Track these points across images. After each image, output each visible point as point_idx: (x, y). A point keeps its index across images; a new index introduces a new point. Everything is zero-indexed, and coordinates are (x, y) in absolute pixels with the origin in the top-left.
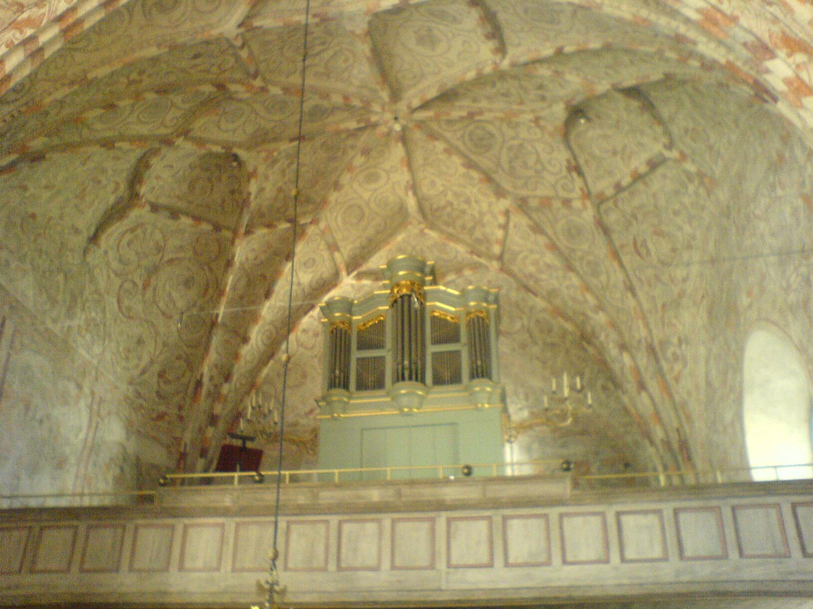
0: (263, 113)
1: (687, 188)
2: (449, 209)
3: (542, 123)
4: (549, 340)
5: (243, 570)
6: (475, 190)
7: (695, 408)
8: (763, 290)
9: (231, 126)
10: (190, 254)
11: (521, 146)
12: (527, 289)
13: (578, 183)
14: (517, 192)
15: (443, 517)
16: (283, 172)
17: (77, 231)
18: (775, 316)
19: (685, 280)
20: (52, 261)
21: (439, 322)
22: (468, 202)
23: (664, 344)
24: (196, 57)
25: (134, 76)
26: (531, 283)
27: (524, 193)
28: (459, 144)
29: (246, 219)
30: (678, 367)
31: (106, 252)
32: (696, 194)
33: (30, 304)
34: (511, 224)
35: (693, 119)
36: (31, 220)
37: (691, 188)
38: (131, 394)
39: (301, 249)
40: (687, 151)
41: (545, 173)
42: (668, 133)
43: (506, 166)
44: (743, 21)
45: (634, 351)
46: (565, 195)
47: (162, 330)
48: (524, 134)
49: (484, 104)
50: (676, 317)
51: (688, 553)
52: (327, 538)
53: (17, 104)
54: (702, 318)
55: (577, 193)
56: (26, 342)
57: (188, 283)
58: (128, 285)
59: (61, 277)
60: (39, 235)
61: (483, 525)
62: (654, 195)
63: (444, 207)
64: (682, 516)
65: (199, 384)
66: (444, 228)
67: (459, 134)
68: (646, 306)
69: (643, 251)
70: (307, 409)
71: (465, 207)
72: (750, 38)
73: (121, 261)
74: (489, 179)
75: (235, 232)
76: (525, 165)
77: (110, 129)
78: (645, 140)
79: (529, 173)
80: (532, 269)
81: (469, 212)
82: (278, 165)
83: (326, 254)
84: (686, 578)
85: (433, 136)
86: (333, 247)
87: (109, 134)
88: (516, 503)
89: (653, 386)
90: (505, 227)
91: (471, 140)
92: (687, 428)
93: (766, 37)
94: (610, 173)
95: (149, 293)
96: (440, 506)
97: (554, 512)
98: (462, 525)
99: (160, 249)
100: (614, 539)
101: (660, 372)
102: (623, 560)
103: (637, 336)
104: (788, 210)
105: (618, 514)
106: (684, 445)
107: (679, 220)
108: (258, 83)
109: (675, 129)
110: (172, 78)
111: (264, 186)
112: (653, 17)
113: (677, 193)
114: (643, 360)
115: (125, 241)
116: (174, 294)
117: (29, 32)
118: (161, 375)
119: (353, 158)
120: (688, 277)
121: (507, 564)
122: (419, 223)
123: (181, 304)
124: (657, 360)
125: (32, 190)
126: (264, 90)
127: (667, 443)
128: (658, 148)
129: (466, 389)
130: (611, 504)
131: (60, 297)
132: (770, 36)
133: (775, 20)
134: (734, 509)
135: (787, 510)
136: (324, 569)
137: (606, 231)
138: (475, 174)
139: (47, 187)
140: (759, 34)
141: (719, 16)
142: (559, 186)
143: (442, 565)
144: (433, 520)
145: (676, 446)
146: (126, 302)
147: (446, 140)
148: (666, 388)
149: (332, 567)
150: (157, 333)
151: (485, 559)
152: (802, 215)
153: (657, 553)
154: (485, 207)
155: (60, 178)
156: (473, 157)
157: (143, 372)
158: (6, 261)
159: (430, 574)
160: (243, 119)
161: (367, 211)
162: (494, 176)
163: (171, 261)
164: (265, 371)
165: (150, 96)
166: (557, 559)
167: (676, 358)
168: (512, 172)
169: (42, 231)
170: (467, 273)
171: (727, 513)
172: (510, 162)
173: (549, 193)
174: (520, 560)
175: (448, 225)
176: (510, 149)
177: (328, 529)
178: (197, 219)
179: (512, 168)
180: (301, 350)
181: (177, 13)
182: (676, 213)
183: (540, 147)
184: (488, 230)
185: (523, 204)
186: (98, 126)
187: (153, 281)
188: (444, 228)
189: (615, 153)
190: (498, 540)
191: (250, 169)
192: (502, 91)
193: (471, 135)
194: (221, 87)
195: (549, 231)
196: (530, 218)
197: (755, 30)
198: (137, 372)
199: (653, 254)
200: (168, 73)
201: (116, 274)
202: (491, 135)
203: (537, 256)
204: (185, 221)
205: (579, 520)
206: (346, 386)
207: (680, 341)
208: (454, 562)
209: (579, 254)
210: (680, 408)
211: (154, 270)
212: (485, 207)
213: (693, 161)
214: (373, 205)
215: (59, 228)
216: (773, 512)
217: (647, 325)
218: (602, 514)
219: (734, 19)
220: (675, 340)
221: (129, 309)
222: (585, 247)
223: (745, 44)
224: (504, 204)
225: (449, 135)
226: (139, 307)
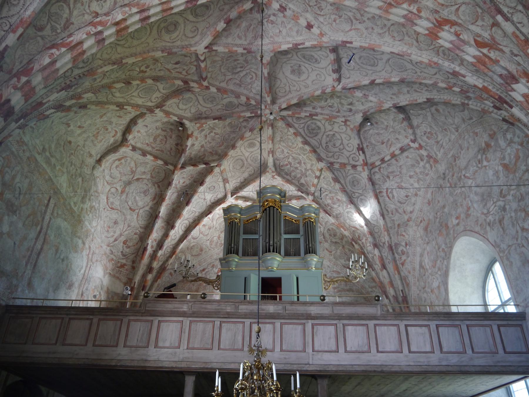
0: (202, 102)
1: (419, 164)
2: (289, 166)
3: (348, 123)
4: (334, 240)
5: (193, 349)
6: (305, 157)
7: (411, 280)
8: (468, 216)
9: (184, 107)
10: (149, 177)
11: (334, 134)
13: (362, 157)
14: (328, 159)
15: (310, 323)
16: (206, 136)
17: (91, 156)
18: (477, 229)
19: (411, 212)
20: (77, 170)
21: (288, 222)
22: (300, 163)
24: (177, 63)
25: (143, 68)
27: (332, 160)
28: (301, 131)
29: (182, 160)
30: (404, 258)
31: (104, 170)
32: (424, 167)
33: (63, 191)
34: (322, 177)
35: (431, 127)
36: (68, 144)
37: (422, 164)
38: (108, 252)
39: (209, 180)
40: (423, 144)
41: (344, 150)
42: (414, 133)
43: (324, 145)
44: (502, 63)
45: (381, 248)
46: (354, 163)
47: (128, 217)
48: (336, 128)
49: (319, 110)
50: (405, 231)
51: (445, 350)
52: (244, 332)
53: (83, 70)
54: (420, 232)
56: (60, 213)
57: (145, 192)
58: (113, 190)
59: (80, 180)
60: (72, 154)
61: (332, 329)
62: (400, 166)
63: (287, 165)
64: (440, 329)
66: (285, 176)
67: (302, 125)
68: (389, 225)
69: (390, 195)
70: (201, 269)
71: (298, 165)
72: (504, 72)
73: (111, 176)
74: (315, 151)
75: (175, 167)
77: (123, 97)
78: (400, 137)
79: (337, 150)
80: (329, 201)
81: (299, 168)
82: (204, 132)
83: (221, 184)
84: (444, 363)
85: (289, 125)
86: (225, 181)
87: (121, 100)
88: (350, 317)
89: (390, 267)
90: (318, 178)
91: (308, 129)
92: (406, 290)
93: (514, 72)
94: (379, 153)
95: (124, 196)
96: (309, 317)
97: (371, 323)
98: (321, 328)
99: (133, 172)
101: (395, 260)
102: (410, 352)
103: (383, 241)
104: (491, 173)
105: (406, 326)
106: (405, 299)
107: (412, 181)
108: (205, 83)
109: (418, 132)
110: (162, 74)
111: (194, 145)
112: (440, 62)
113: (413, 166)
114: (386, 252)
115: (114, 166)
116: (137, 198)
117: (100, 28)
118: (125, 243)
119: (245, 132)
120: (413, 210)
121: (346, 351)
122: (273, 172)
123: (140, 204)
124: (393, 254)
125: (72, 127)
126: (207, 88)
127: (396, 298)
128: (407, 141)
129: (303, 259)
130: (402, 320)
131: (79, 191)
132: (517, 71)
133: (519, 64)
134: (468, 326)
135: (495, 328)
136: (242, 350)
138: (307, 148)
139: (80, 127)
140: (511, 70)
141: (487, 60)
142: (350, 159)
143: (309, 350)
144: (304, 324)
145: (400, 299)
146: (111, 200)
147: (295, 129)
148: (397, 269)
149: (246, 349)
150: (125, 219)
151: (334, 348)
152: (501, 175)
153: (428, 349)
154: (309, 167)
155: (87, 123)
156: (307, 138)
157: (116, 240)
158: (54, 165)
159: (303, 354)
160: (191, 104)
161: (246, 163)
162: (318, 150)
163: (138, 179)
164: (182, 246)
165: (150, 81)
166: (374, 349)
167: (403, 253)
168: (327, 148)
169: (73, 152)
171: (464, 328)
172: (327, 143)
173: (345, 161)
174: (353, 349)
175: (287, 175)
176: (328, 136)
177: (244, 326)
178: (156, 157)
179: (327, 146)
180: (201, 235)
181: (174, 35)
182: (411, 177)
183: (343, 136)
184: (308, 179)
185: (330, 166)
186: (118, 94)
187: (127, 189)
188: (285, 176)
189: (383, 143)
190: (340, 338)
191: (190, 132)
192: (330, 104)
193: (308, 126)
194: (186, 82)
195: (343, 182)
196: (333, 173)
197: (508, 68)
198: (112, 239)
199: (396, 198)
200: (160, 70)
201: (108, 183)
202: (319, 128)
203: (333, 195)
204: (149, 157)
206: (237, 254)
207: (406, 245)
208: (316, 349)
209: (357, 194)
210: (403, 280)
211: (129, 183)
212: (309, 167)
213: (425, 150)
214: (249, 160)
215: (82, 152)
216: (488, 329)
217: (389, 235)
218: (398, 326)
219: (497, 62)
220: (404, 244)
221: (112, 203)
222: (360, 192)
223: (501, 76)
224: (321, 165)
225: (296, 126)
226: (117, 203)
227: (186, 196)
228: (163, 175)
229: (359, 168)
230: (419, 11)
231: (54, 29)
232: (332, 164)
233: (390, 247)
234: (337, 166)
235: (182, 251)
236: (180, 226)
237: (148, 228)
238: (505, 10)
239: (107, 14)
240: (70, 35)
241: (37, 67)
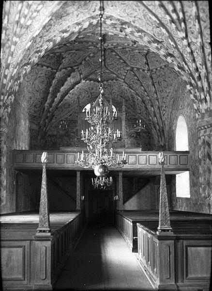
12: (130, 87)
18: (185, 116)
19: (169, 93)
23: (162, 106)
26: (131, 86)
27: (133, 66)
30: (164, 112)
39: (72, 74)
43: (129, 59)
55: (146, 69)
65: (44, 108)
68: (159, 97)
76: (134, 60)
86: (81, 74)
88: (130, 153)
89: (158, 115)
97: (137, 155)
100: (148, 160)
106: (163, 131)
114: (156, 109)
118: (35, 106)
127: (159, 130)
137: (152, 78)
166: (137, 164)
170: (114, 81)
178: (48, 67)
204: (45, 67)
205: (142, 157)
217: (158, 101)
225: (116, 51)
227: (62, 82)
228: (50, 74)
229: (146, 72)
230: (161, 48)
231: (25, 59)
232: (133, 68)
233: (159, 108)
234: (135, 69)
235: (61, 107)
236: (59, 95)
237: (45, 99)
238: (186, 60)
239: (41, 46)
240: (30, 59)
241: (22, 75)
